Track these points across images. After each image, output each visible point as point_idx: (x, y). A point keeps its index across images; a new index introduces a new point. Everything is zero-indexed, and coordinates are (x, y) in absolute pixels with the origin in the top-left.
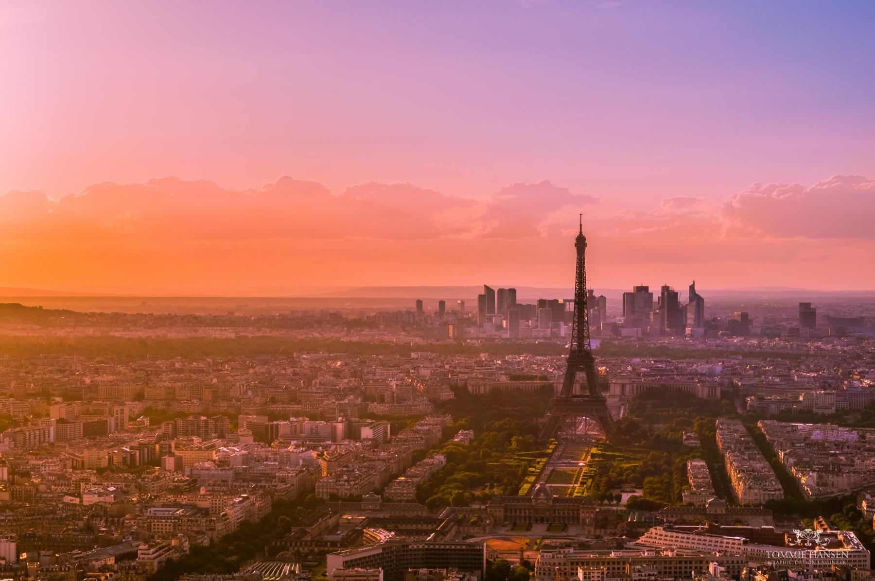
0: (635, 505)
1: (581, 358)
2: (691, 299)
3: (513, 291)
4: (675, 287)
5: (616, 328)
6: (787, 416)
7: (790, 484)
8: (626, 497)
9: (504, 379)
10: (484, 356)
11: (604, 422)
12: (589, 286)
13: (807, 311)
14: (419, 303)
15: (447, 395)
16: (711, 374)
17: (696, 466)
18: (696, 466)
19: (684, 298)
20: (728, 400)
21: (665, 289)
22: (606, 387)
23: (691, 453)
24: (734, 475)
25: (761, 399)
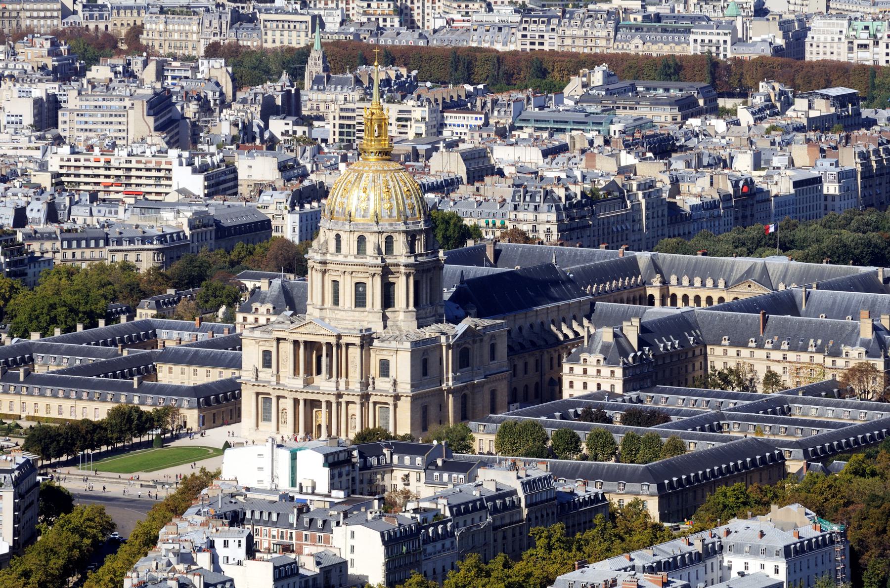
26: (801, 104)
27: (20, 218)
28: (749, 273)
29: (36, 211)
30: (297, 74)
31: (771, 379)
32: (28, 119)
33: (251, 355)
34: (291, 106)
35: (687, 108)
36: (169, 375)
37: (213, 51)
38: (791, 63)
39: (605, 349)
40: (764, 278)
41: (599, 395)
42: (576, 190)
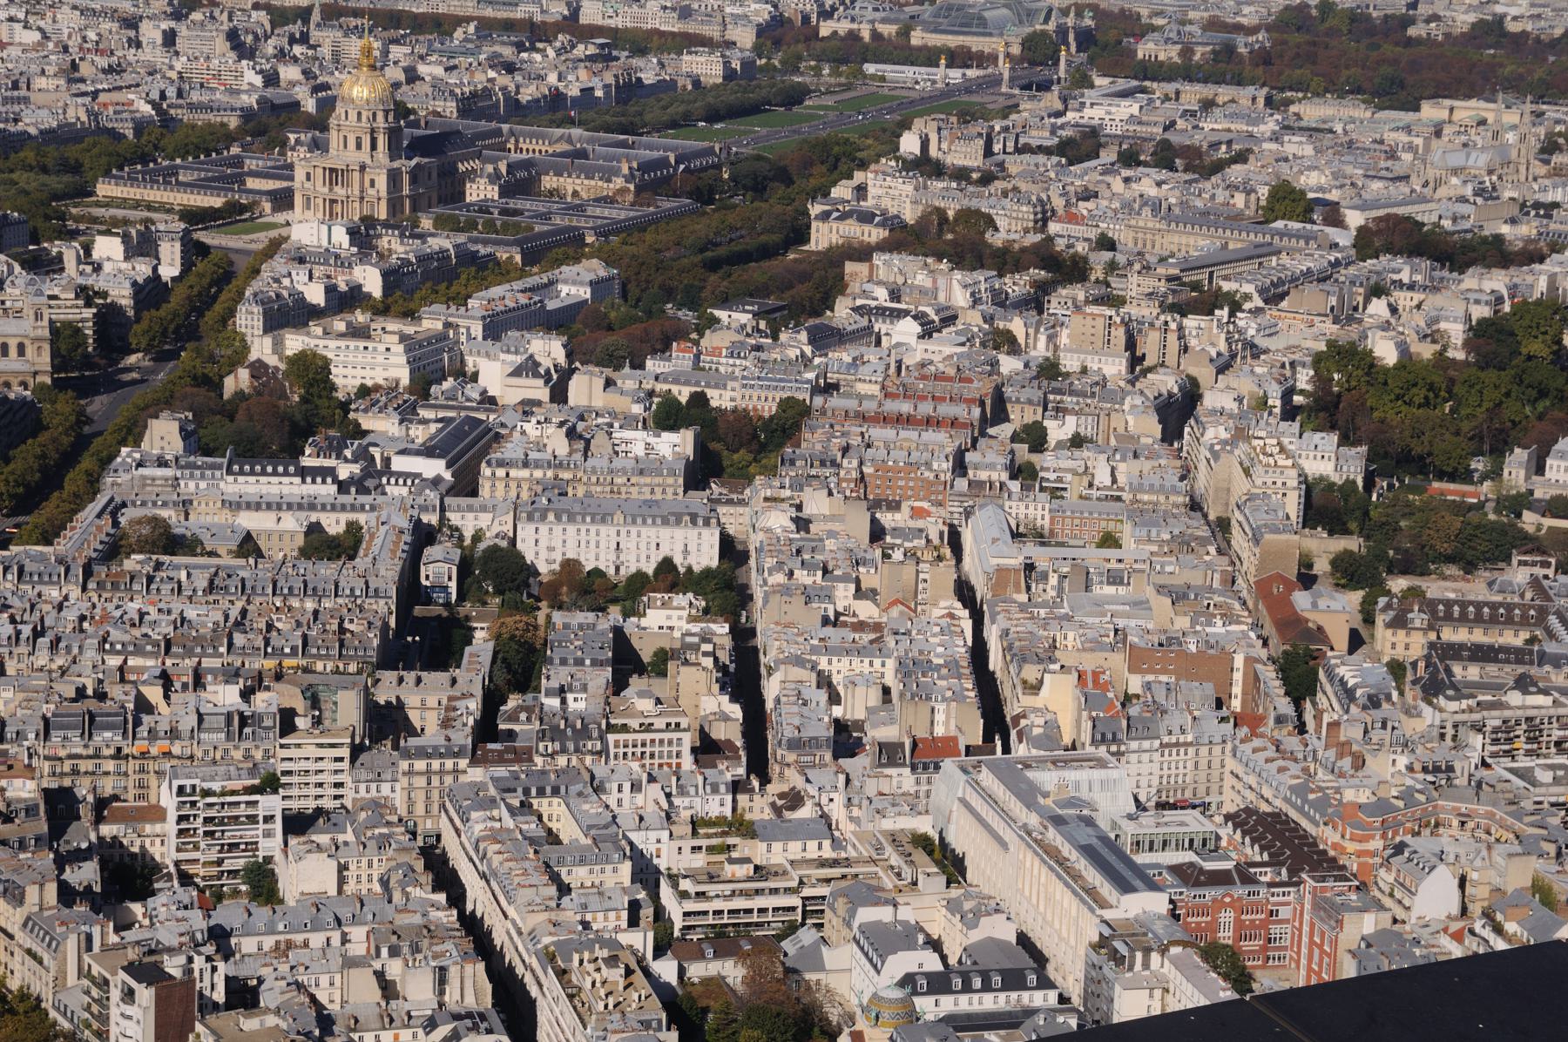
26: (581, 47)
27: (163, 96)
28: (561, 137)
29: (171, 92)
30: (306, 21)
31: (575, 194)
32: (159, 41)
33: (299, 174)
34: (304, 39)
35: (520, 47)
36: (252, 183)
38: (571, 23)
39: (489, 176)
40: (570, 140)
41: (486, 200)
42: (466, 90)
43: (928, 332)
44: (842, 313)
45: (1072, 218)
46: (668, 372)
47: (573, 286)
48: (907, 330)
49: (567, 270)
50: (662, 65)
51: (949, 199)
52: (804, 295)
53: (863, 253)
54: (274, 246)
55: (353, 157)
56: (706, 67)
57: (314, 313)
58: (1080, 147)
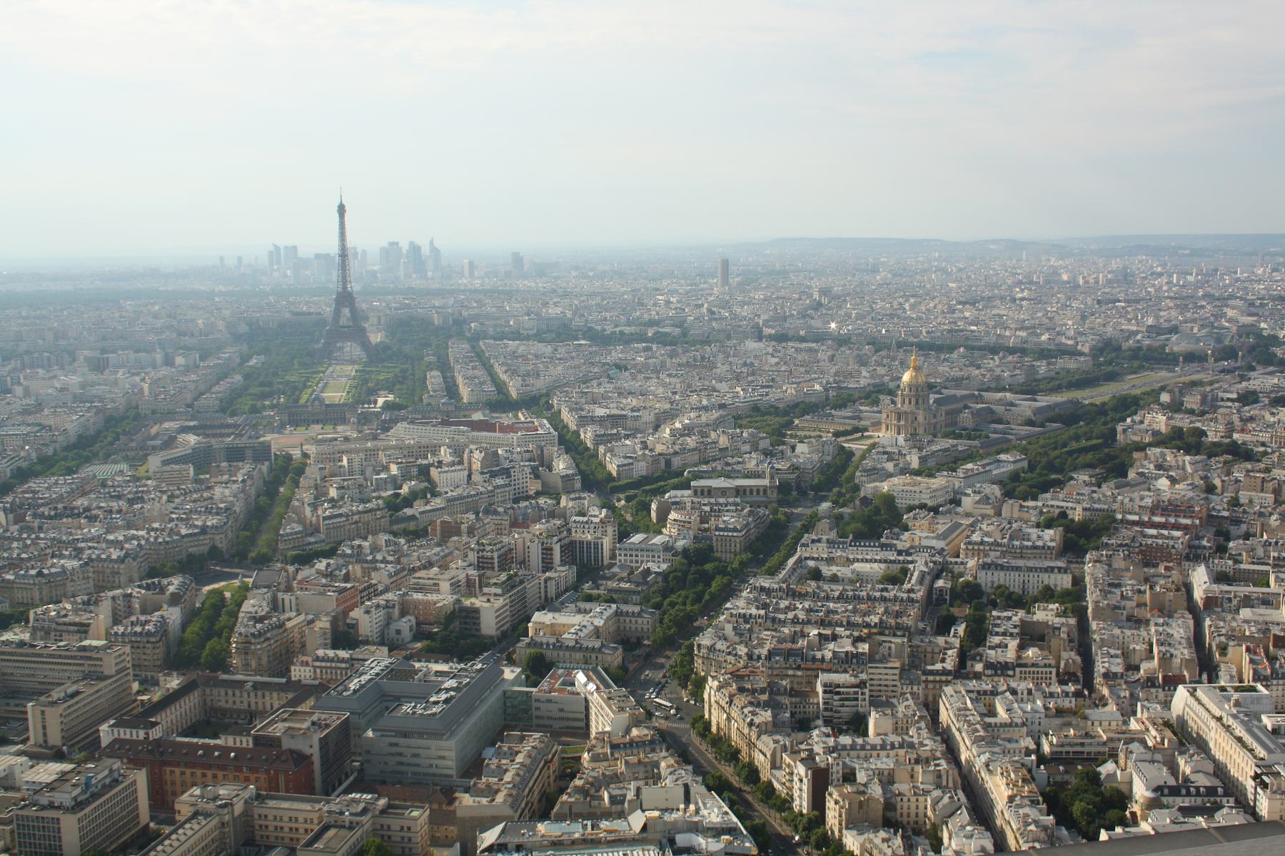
0: (388, 406)
1: (345, 298)
2: (431, 251)
3: (295, 248)
4: (419, 242)
5: (374, 273)
6: (500, 337)
7: (500, 387)
8: (381, 401)
9: (288, 315)
10: (272, 299)
11: (365, 344)
12: (350, 242)
13: (517, 259)
14: (222, 258)
15: (243, 328)
16: (443, 307)
17: (434, 379)
18: (434, 379)
19: (426, 250)
20: (456, 327)
21: (412, 244)
22: (367, 319)
23: (430, 367)
24: (460, 380)
25: (482, 324)
27: (828, 383)
35: (984, 357)
37: (868, 344)
43: (1173, 481)
44: (1132, 475)
45: (1243, 431)
46: (1052, 501)
47: (1009, 461)
48: (1163, 483)
49: (1003, 457)
50: (1049, 364)
51: (1184, 422)
52: (1114, 465)
53: (1141, 448)
54: (873, 446)
55: (906, 408)
56: (1071, 364)
57: (891, 475)
58: (1248, 398)
